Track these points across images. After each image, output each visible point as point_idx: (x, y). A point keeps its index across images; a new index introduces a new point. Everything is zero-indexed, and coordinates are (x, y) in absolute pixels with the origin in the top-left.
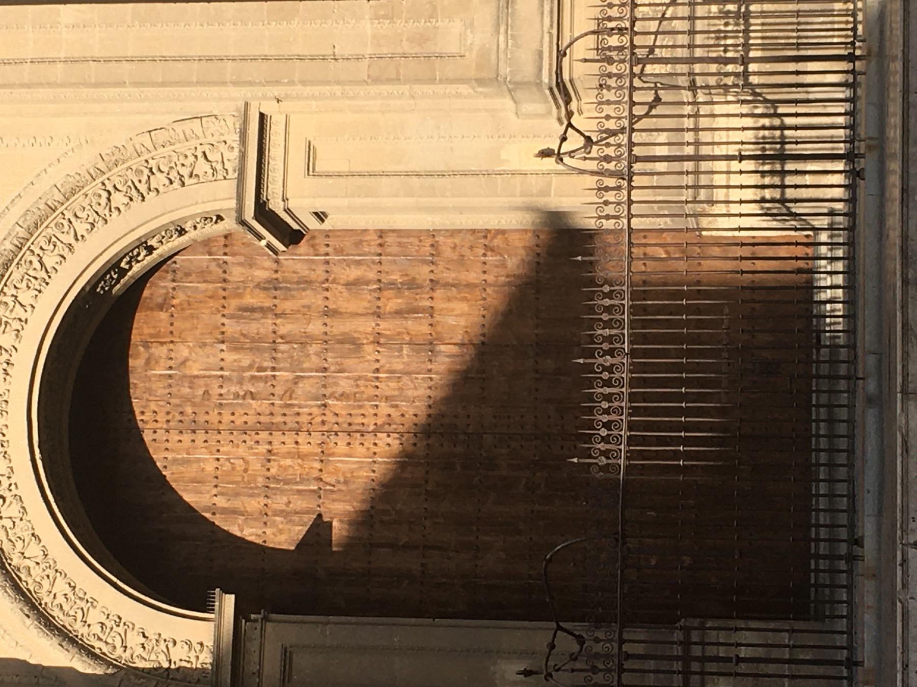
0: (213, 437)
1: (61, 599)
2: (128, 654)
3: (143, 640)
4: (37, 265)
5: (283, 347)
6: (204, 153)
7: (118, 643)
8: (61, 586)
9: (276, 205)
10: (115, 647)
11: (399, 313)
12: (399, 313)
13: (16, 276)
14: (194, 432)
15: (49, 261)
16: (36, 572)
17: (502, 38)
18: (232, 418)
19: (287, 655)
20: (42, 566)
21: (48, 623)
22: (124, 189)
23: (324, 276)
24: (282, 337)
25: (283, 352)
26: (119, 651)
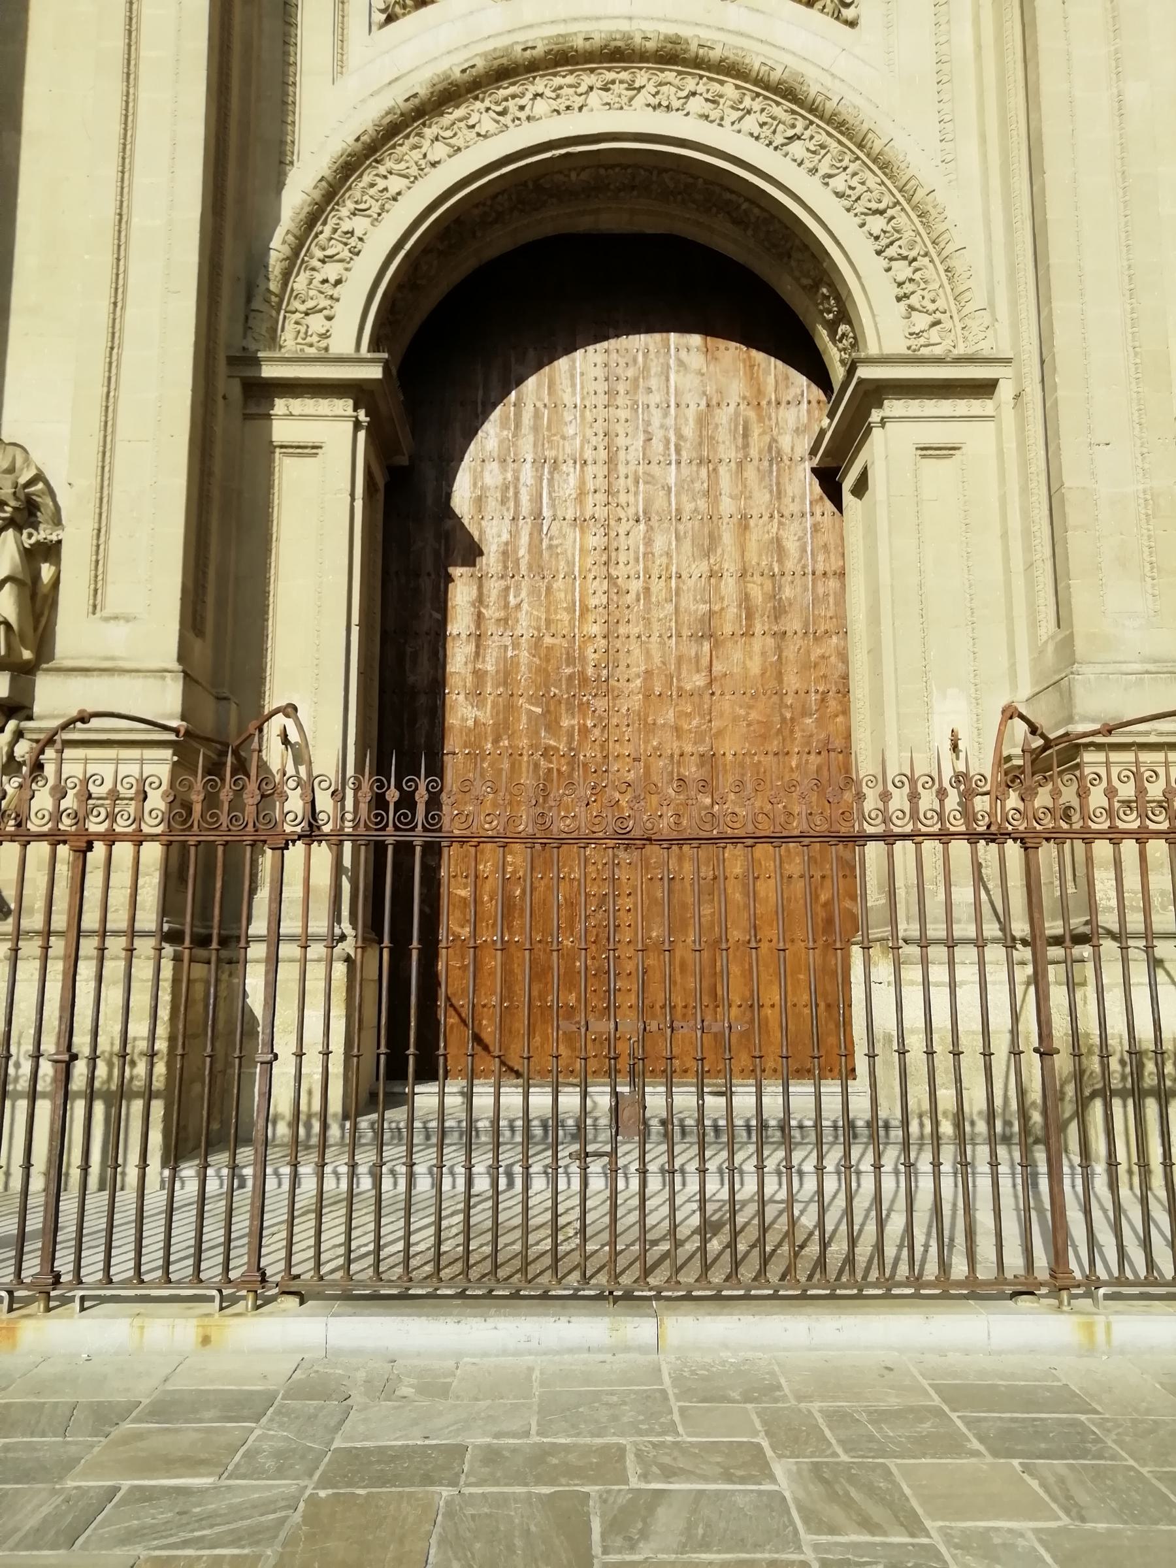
0: (602, 399)
1: (380, 186)
2: (315, 263)
3: (332, 280)
4: (790, 133)
5: (704, 472)
6: (938, 323)
7: (329, 252)
8: (395, 184)
9: (875, 416)
10: (324, 249)
11: (745, 599)
12: (746, 598)
13: (777, 111)
14: (607, 379)
15: (797, 149)
16: (416, 155)
17: (1137, 667)
18: (622, 420)
19: (310, 450)
20: (422, 162)
21: (349, 168)
22: (889, 228)
23: (786, 514)
24: (714, 470)
25: (697, 472)
26: (319, 254)
